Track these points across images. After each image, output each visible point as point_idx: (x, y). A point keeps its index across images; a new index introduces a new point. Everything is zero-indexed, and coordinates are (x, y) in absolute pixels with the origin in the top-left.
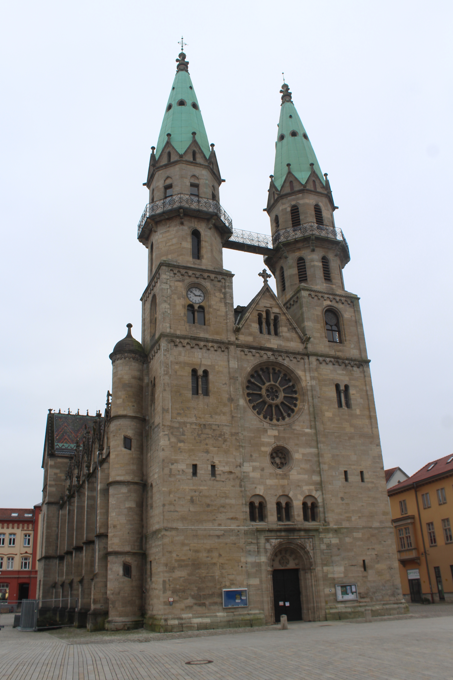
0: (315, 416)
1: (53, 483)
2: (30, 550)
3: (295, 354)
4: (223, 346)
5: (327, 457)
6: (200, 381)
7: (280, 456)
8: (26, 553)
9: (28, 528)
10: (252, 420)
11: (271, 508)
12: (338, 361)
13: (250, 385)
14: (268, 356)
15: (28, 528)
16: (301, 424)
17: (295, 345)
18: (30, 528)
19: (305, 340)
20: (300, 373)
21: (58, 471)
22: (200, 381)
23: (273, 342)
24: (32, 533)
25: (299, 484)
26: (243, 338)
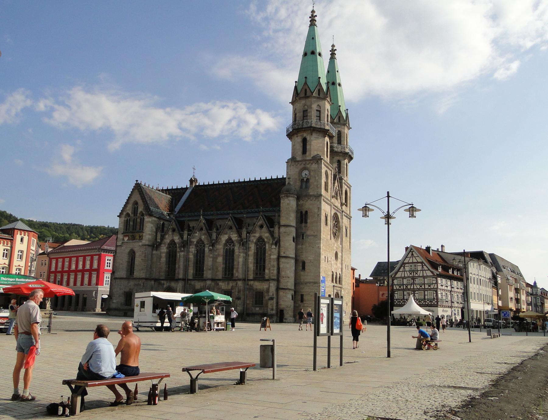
1: (150, 233)
2: (7, 262)
8: (5, 264)
9: (7, 244)
15: (7, 244)
18: (9, 245)
21: (152, 225)
24: (9, 248)
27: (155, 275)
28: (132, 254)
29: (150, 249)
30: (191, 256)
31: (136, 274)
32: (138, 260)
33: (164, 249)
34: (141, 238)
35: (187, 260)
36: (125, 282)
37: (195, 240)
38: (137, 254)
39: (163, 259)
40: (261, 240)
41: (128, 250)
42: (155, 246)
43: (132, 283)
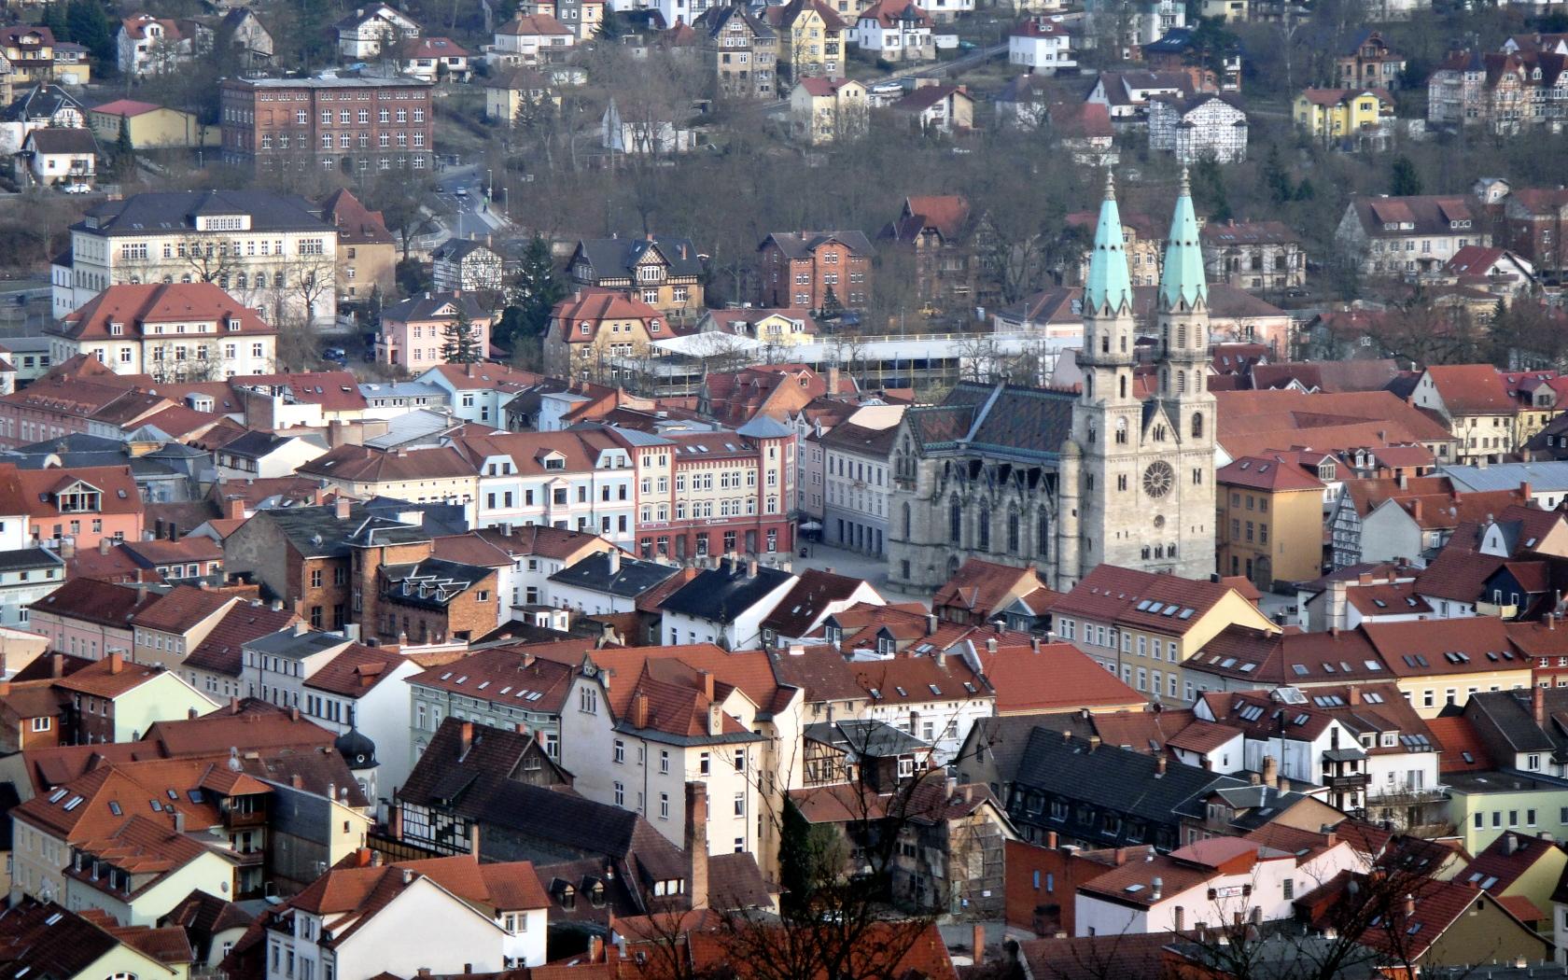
0: (1179, 493)
3: (1171, 454)
4: (1135, 458)
5: (1184, 519)
6: (1122, 483)
7: (1160, 520)
10: (1145, 498)
11: (1152, 552)
12: (1197, 453)
13: (1147, 477)
14: (1157, 458)
16: (1171, 499)
17: (1174, 446)
19: (1178, 442)
20: (1173, 465)
22: (1122, 483)
23: (1160, 447)
25: (1167, 536)
26: (1145, 448)
27: (937, 541)
28: (906, 507)
29: (927, 504)
30: (975, 518)
31: (914, 537)
32: (913, 518)
33: (946, 503)
34: (915, 488)
35: (970, 522)
36: (900, 547)
37: (978, 497)
38: (913, 510)
39: (946, 518)
40: (1042, 507)
41: (901, 503)
42: (934, 498)
43: (909, 548)
